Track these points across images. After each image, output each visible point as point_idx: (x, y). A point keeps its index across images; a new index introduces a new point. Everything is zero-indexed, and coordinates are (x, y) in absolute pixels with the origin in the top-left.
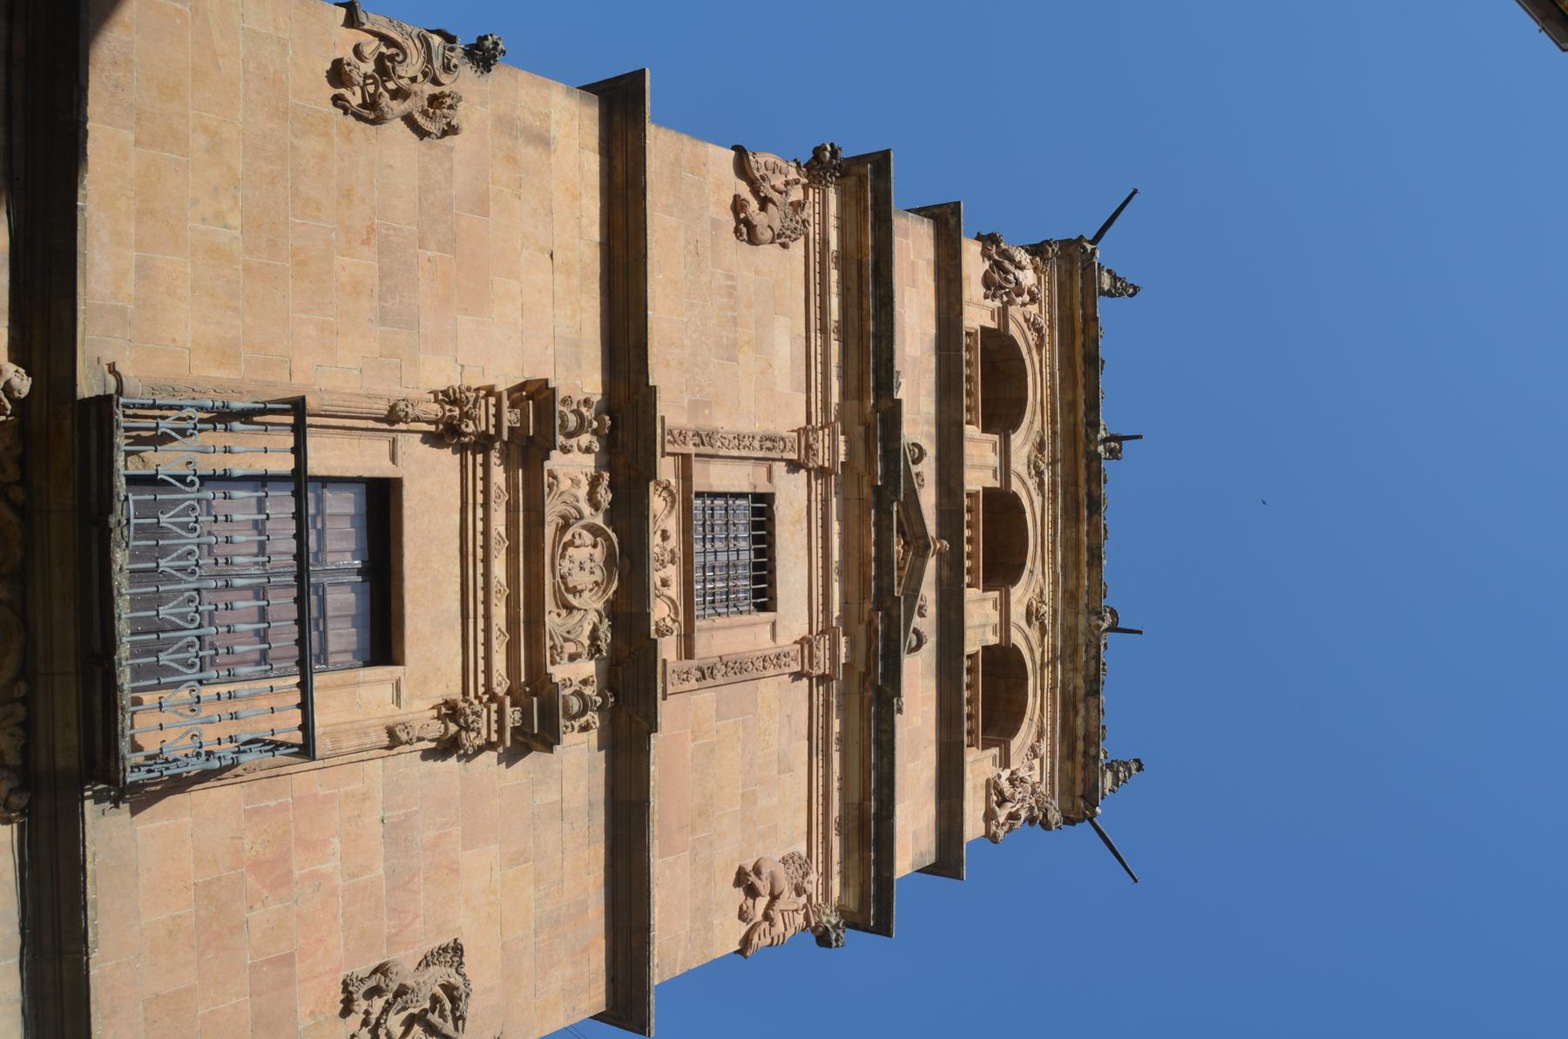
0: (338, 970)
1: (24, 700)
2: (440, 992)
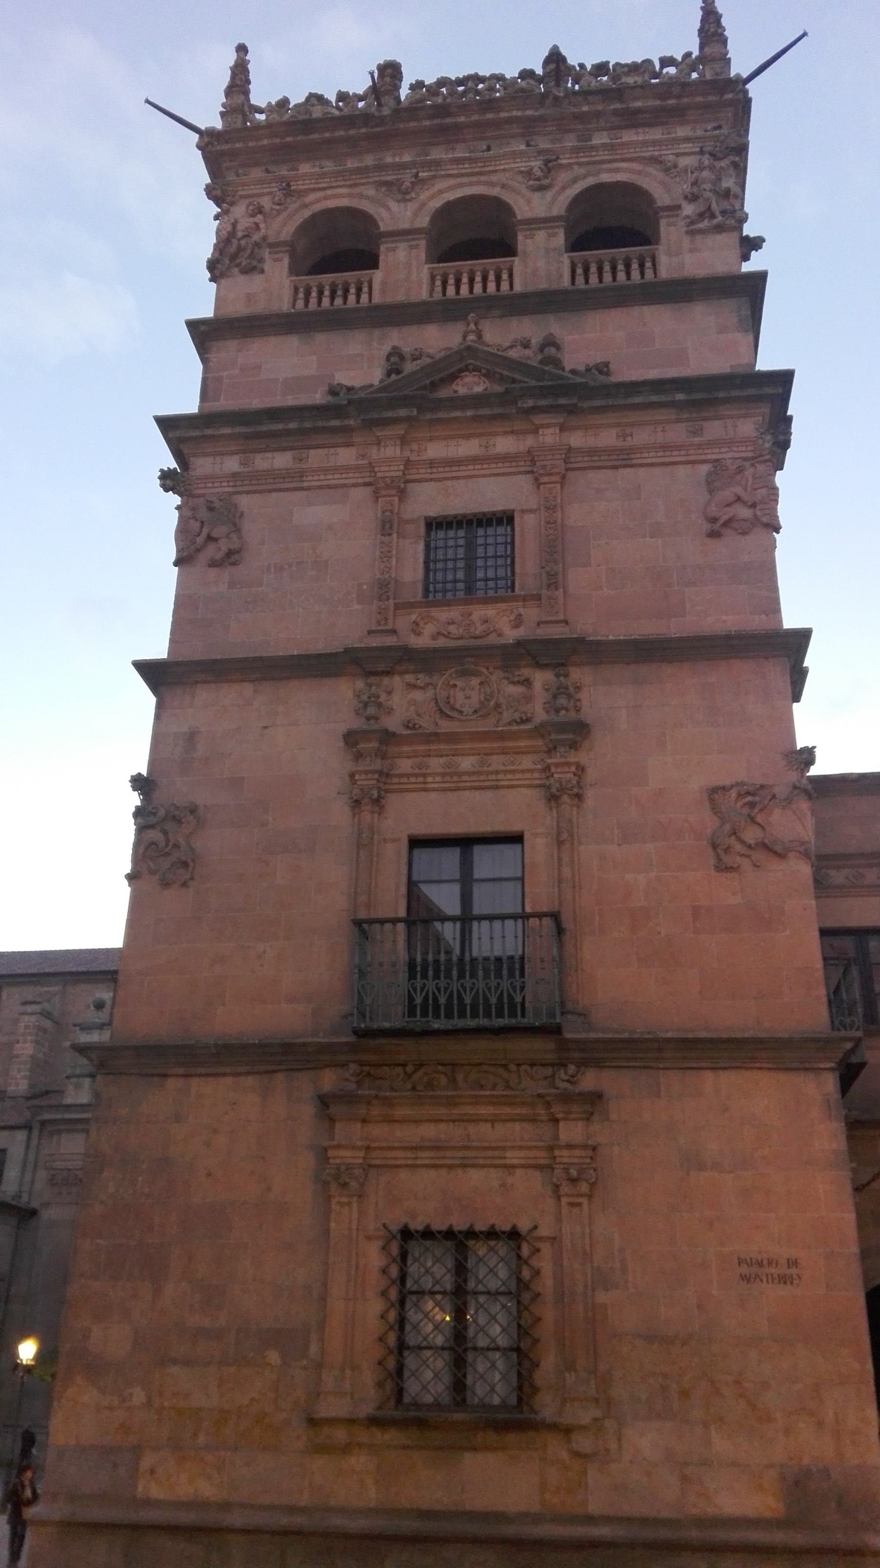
1: (519, 1065)
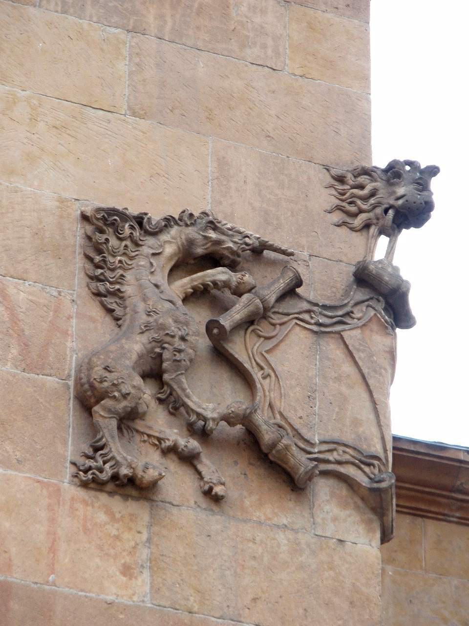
0: (58, 492)
2: (185, 283)
